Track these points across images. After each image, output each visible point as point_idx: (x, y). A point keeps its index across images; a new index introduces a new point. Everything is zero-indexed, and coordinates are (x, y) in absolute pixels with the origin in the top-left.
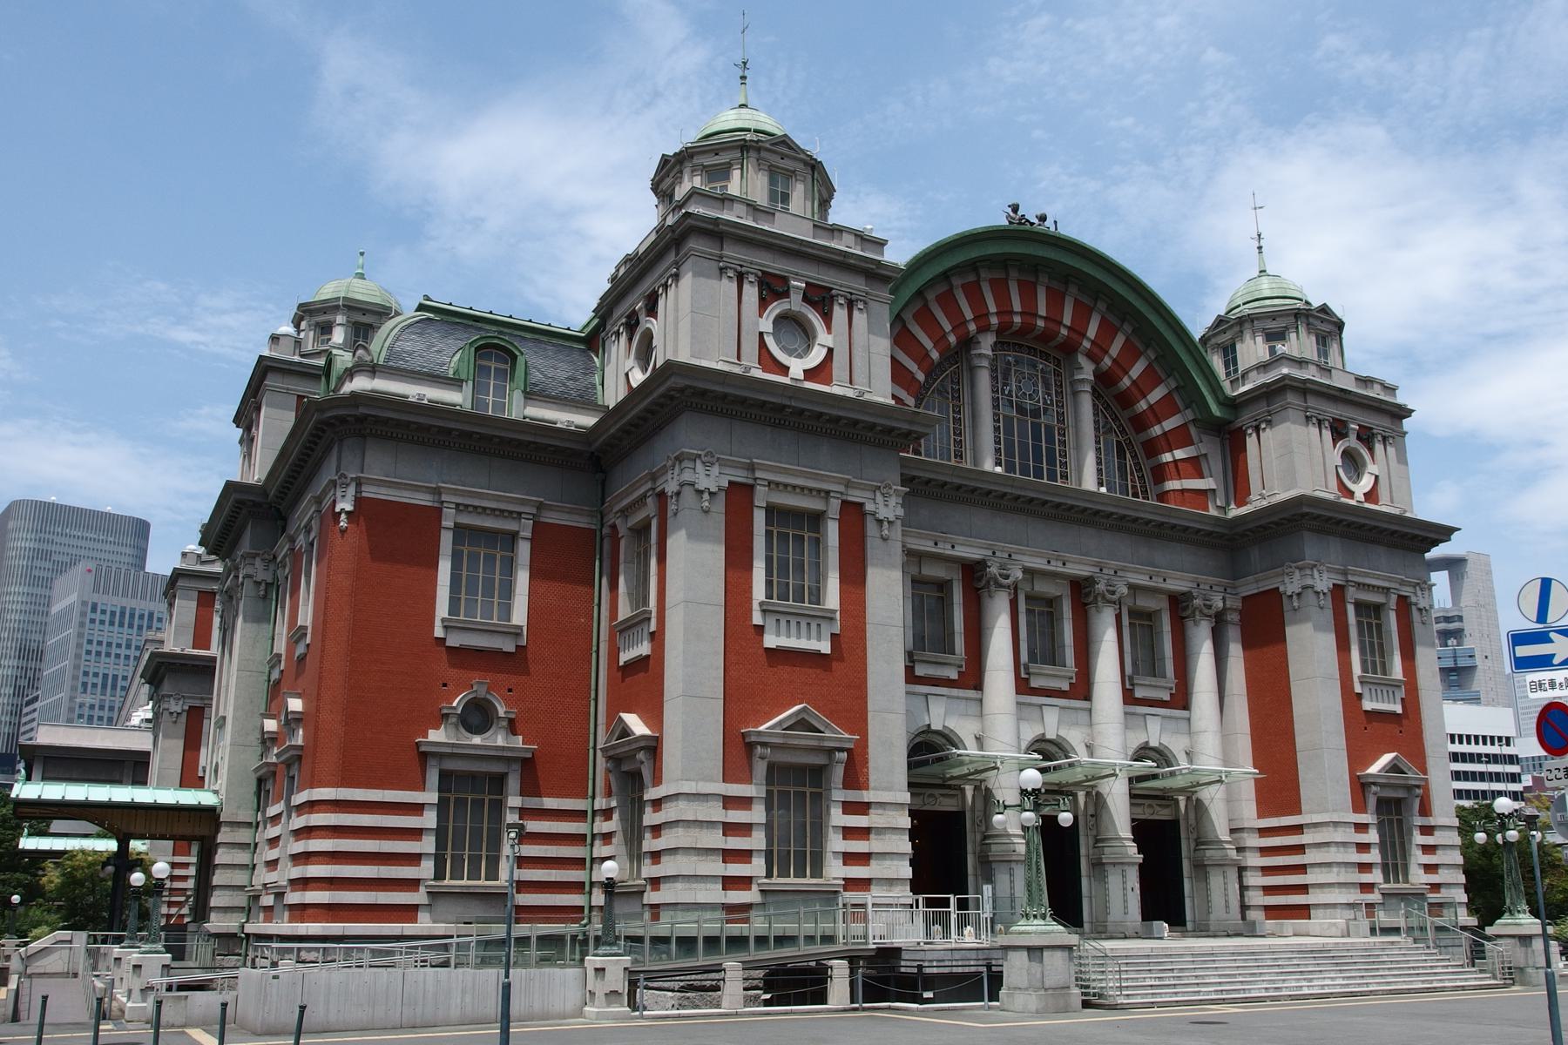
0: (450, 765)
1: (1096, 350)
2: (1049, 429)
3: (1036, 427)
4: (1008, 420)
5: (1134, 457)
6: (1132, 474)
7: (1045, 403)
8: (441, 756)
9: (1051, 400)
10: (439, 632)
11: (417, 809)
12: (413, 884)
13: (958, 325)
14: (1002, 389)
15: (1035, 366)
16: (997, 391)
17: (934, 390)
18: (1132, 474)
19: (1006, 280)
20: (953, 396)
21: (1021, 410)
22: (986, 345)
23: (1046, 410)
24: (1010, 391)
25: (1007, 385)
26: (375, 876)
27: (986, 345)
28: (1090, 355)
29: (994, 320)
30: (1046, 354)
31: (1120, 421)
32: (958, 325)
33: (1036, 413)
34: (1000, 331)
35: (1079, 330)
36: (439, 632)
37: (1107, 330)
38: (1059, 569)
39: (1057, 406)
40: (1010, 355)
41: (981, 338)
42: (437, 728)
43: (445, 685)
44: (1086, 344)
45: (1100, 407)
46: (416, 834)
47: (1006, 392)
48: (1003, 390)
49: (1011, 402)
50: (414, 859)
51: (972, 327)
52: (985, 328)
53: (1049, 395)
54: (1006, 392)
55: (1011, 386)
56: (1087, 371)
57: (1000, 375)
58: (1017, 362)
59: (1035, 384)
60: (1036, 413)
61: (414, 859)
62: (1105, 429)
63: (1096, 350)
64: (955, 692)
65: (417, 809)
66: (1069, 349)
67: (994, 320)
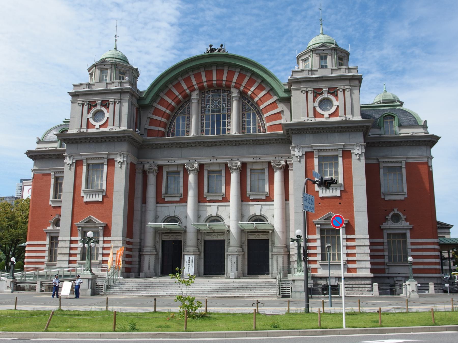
0: (52, 235)
1: (237, 85)
2: (224, 116)
7: (223, 106)
8: (50, 233)
9: (226, 106)
10: (50, 203)
11: (44, 245)
12: (43, 263)
13: (182, 91)
14: (206, 107)
15: (220, 96)
16: (204, 108)
17: (180, 113)
19: (200, 73)
20: (187, 113)
21: (213, 111)
22: (195, 95)
23: (223, 109)
24: (209, 107)
25: (207, 105)
27: (195, 95)
28: (235, 87)
29: (196, 87)
30: (225, 90)
31: (254, 105)
32: (182, 91)
33: (219, 111)
34: (202, 89)
35: (229, 80)
36: (50, 203)
37: (241, 77)
38: (214, 162)
39: (228, 106)
40: (210, 95)
41: (193, 93)
42: (49, 226)
43: (52, 216)
44: (233, 84)
45: (246, 102)
46: (44, 251)
47: (208, 107)
48: (206, 107)
49: (209, 110)
50: (43, 257)
51: (188, 91)
52: (194, 90)
53: (224, 104)
54: (208, 107)
56: (235, 93)
57: (202, 102)
58: (212, 96)
59: (219, 102)
60: (219, 111)
61: (43, 257)
62: (248, 110)
63: (237, 85)
64: (178, 204)
65: (44, 245)
66: (228, 89)
67: (196, 87)
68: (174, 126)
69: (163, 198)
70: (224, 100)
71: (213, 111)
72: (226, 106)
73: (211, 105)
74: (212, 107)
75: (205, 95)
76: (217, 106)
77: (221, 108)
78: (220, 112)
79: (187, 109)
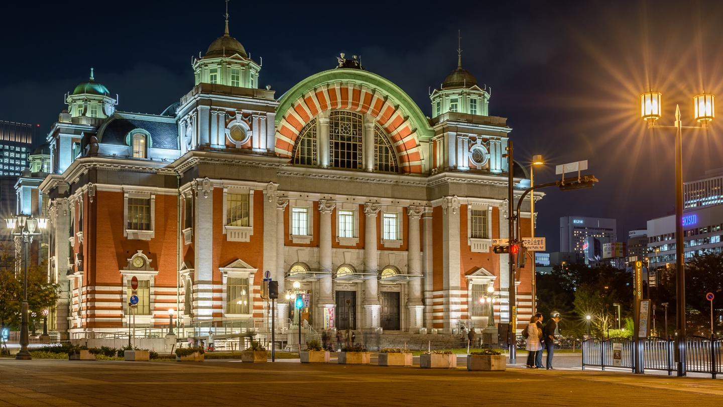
2: (355, 146)
3: (349, 145)
4: (337, 144)
5: (393, 152)
6: (391, 159)
7: (353, 134)
9: (357, 133)
18: (391, 159)
24: (338, 133)
25: (337, 129)
26: (110, 311)
39: (359, 135)
48: (335, 131)
55: (339, 129)
59: (350, 127)
60: (349, 139)
68: (298, 150)
69: (290, 239)
70: (355, 126)
71: (343, 138)
72: (356, 135)
73: (340, 130)
74: (341, 133)
76: (347, 133)
77: (352, 135)
78: (350, 141)
79: (313, 130)
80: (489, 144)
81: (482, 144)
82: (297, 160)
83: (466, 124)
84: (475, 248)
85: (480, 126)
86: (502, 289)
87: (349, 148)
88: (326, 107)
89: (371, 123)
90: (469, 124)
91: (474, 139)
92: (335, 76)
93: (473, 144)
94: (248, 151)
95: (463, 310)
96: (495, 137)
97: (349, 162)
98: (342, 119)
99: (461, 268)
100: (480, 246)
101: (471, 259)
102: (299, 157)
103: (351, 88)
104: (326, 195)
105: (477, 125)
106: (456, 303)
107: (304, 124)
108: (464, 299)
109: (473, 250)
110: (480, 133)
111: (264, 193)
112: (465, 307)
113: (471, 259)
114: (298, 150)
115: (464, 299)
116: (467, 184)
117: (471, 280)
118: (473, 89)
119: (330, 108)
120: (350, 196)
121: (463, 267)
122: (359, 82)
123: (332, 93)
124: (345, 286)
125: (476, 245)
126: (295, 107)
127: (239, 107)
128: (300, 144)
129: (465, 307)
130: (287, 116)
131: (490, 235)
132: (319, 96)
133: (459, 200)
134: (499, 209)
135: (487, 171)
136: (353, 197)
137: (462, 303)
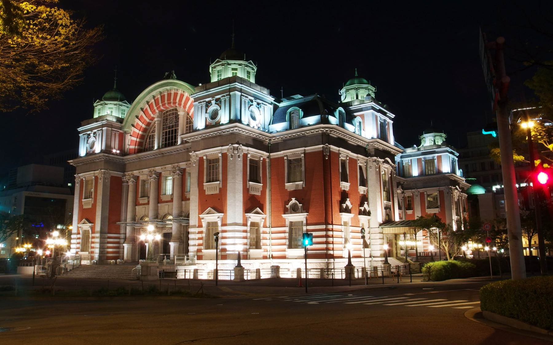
2: (176, 130)
7: (175, 123)
24: (167, 125)
25: (166, 123)
59: (173, 119)
75: (166, 115)
80: (221, 102)
81: (216, 104)
82: (147, 149)
83: (205, 92)
84: (208, 191)
85: (211, 90)
86: (228, 224)
87: (172, 133)
88: (155, 111)
89: (181, 113)
90: (203, 92)
91: (209, 102)
92: (152, 90)
93: (210, 106)
94: (94, 153)
95: (199, 245)
96: (225, 94)
97: (172, 142)
98: (170, 115)
99: (199, 210)
100: (211, 188)
101: (206, 201)
102: (147, 147)
103: (166, 94)
104: (150, 168)
105: (209, 91)
106: (193, 239)
107: (144, 126)
108: (200, 236)
109: (207, 193)
110: (213, 96)
111: (98, 176)
112: (201, 242)
113: (206, 201)
114: (147, 143)
115: (200, 236)
116: (202, 139)
117: (203, 219)
118: (216, 63)
119: (157, 111)
120: (162, 167)
121: (200, 208)
122: (168, 88)
123: (156, 101)
124: (168, 229)
125: (209, 188)
126: (139, 117)
127: (91, 130)
128: (148, 139)
129: (201, 242)
130: (135, 124)
131: (221, 178)
132: (150, 106)
133: (197, 156)
134: (228, 153)
135: (218, 124)
136: (164, 166)
137: (199, 239)
